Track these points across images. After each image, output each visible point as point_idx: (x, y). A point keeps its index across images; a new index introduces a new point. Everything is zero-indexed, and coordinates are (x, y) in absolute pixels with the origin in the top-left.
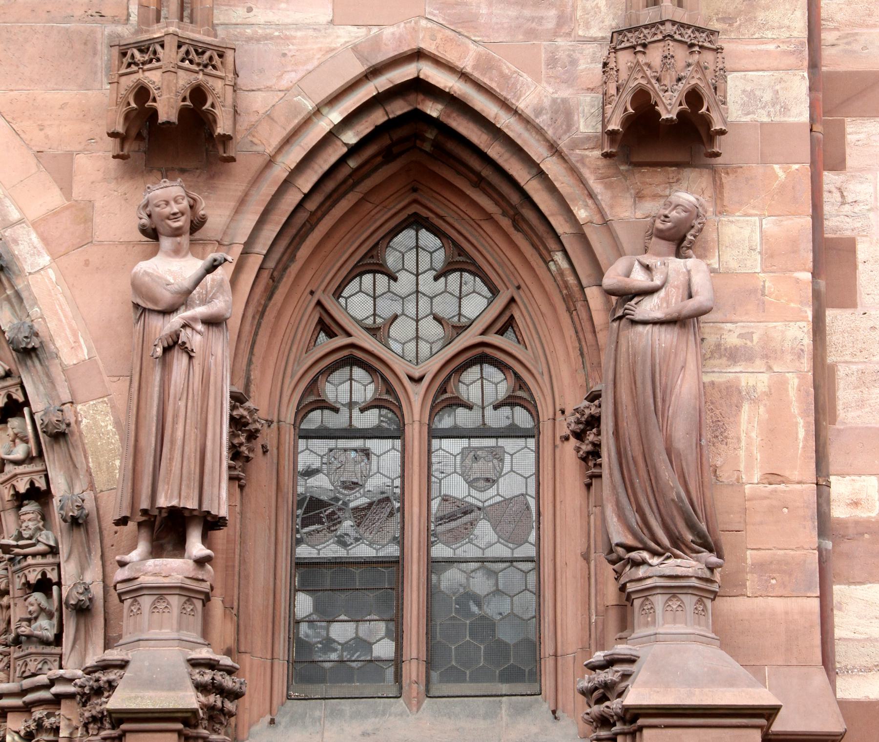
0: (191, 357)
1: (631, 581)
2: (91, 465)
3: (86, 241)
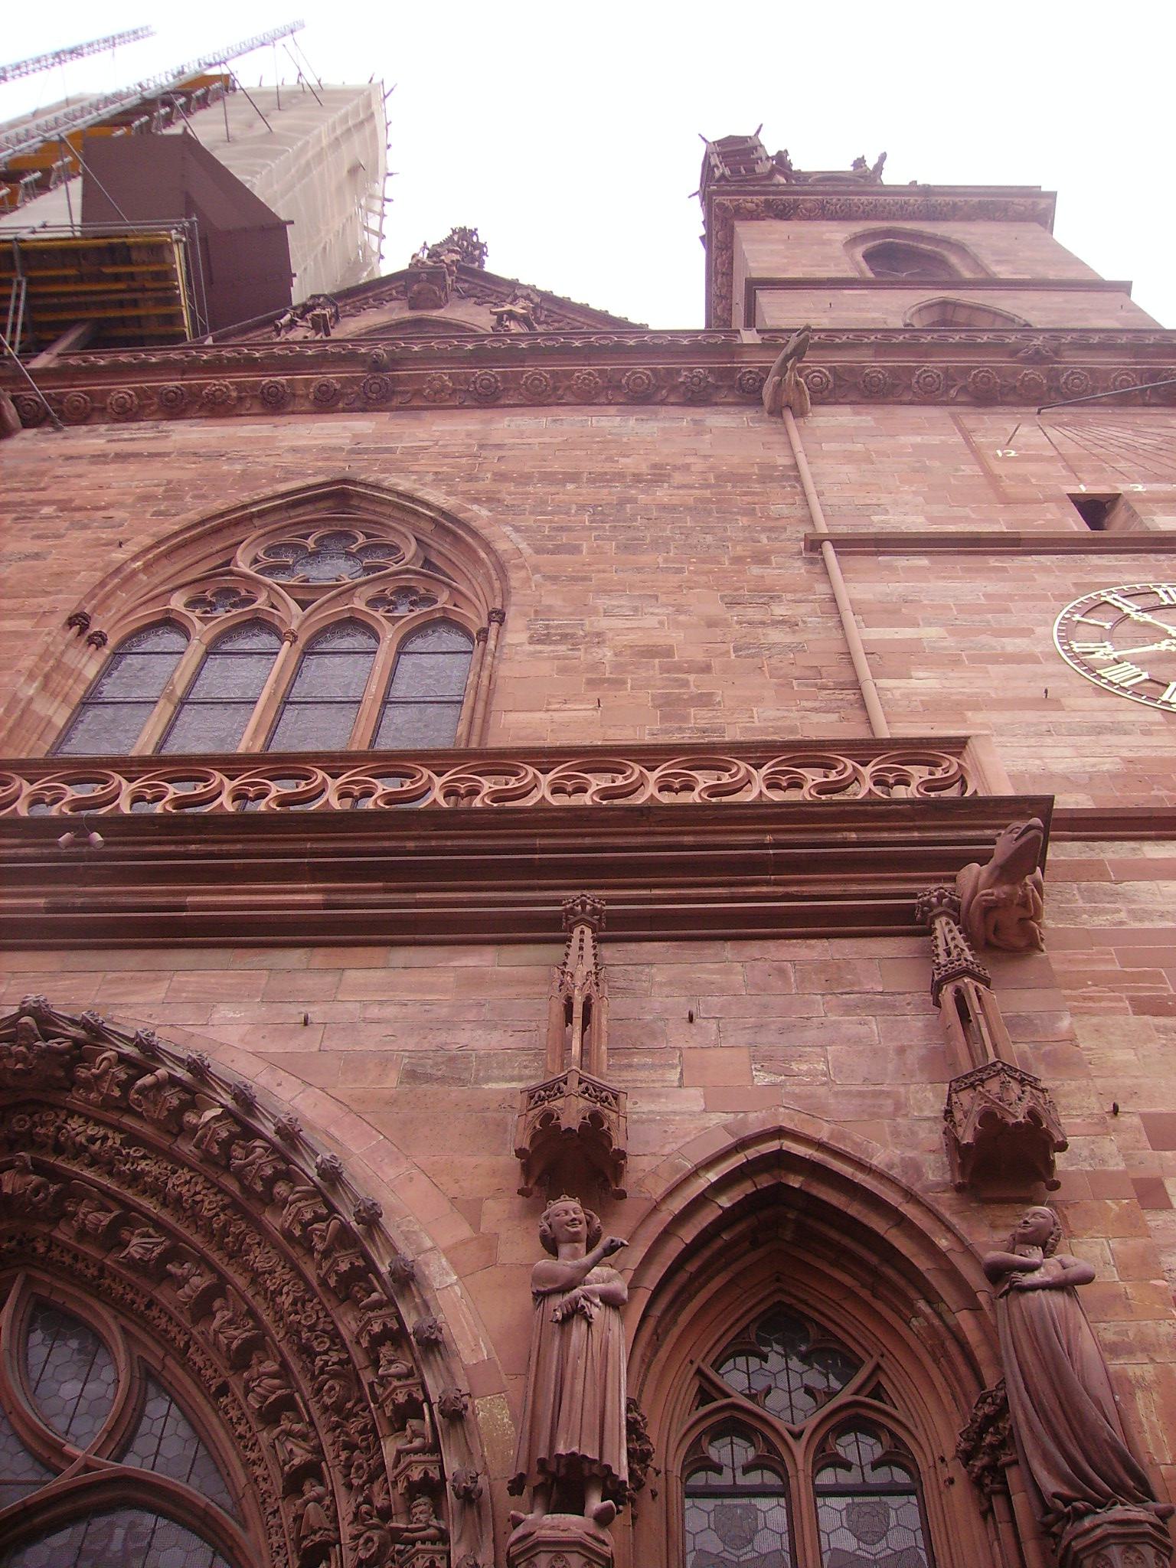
1: (1075, 1538)
2: (486, 1454)
3: (491, 1263)
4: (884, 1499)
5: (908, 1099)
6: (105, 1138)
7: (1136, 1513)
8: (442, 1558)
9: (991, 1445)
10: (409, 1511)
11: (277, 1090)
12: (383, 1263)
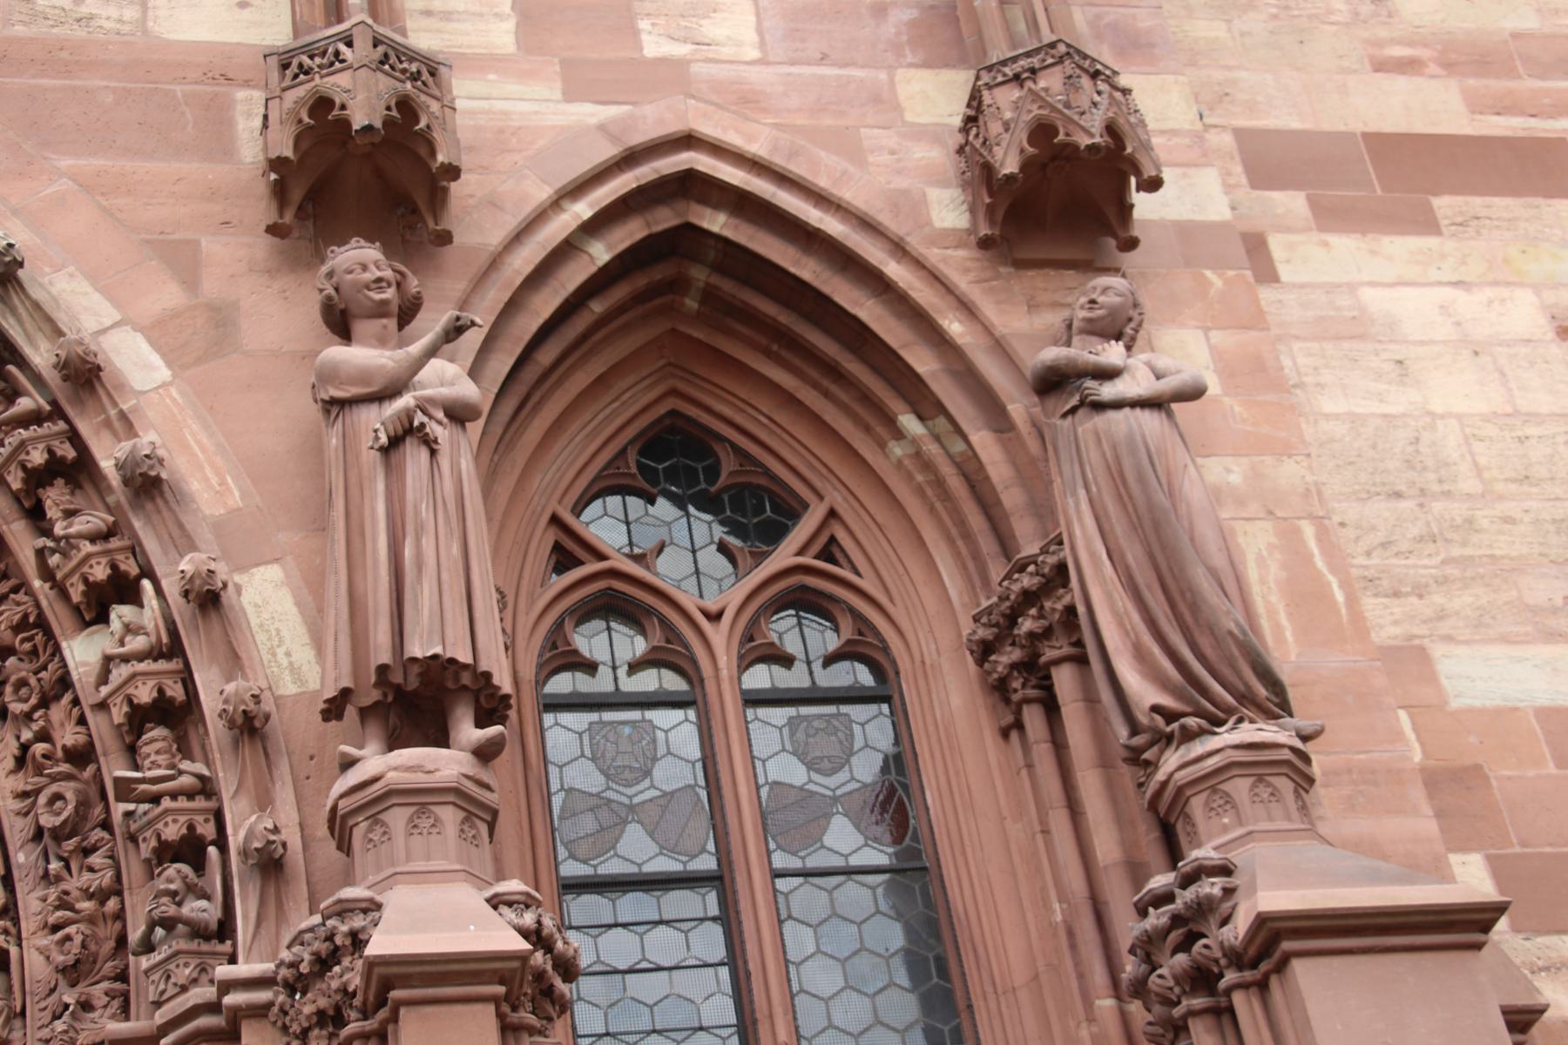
0: (433, 453)
4: (844, 709)
7: (1267, 732)
8: (206, 821)
9: (1031, 635)
10: (132, 750)
12: (36, 348)
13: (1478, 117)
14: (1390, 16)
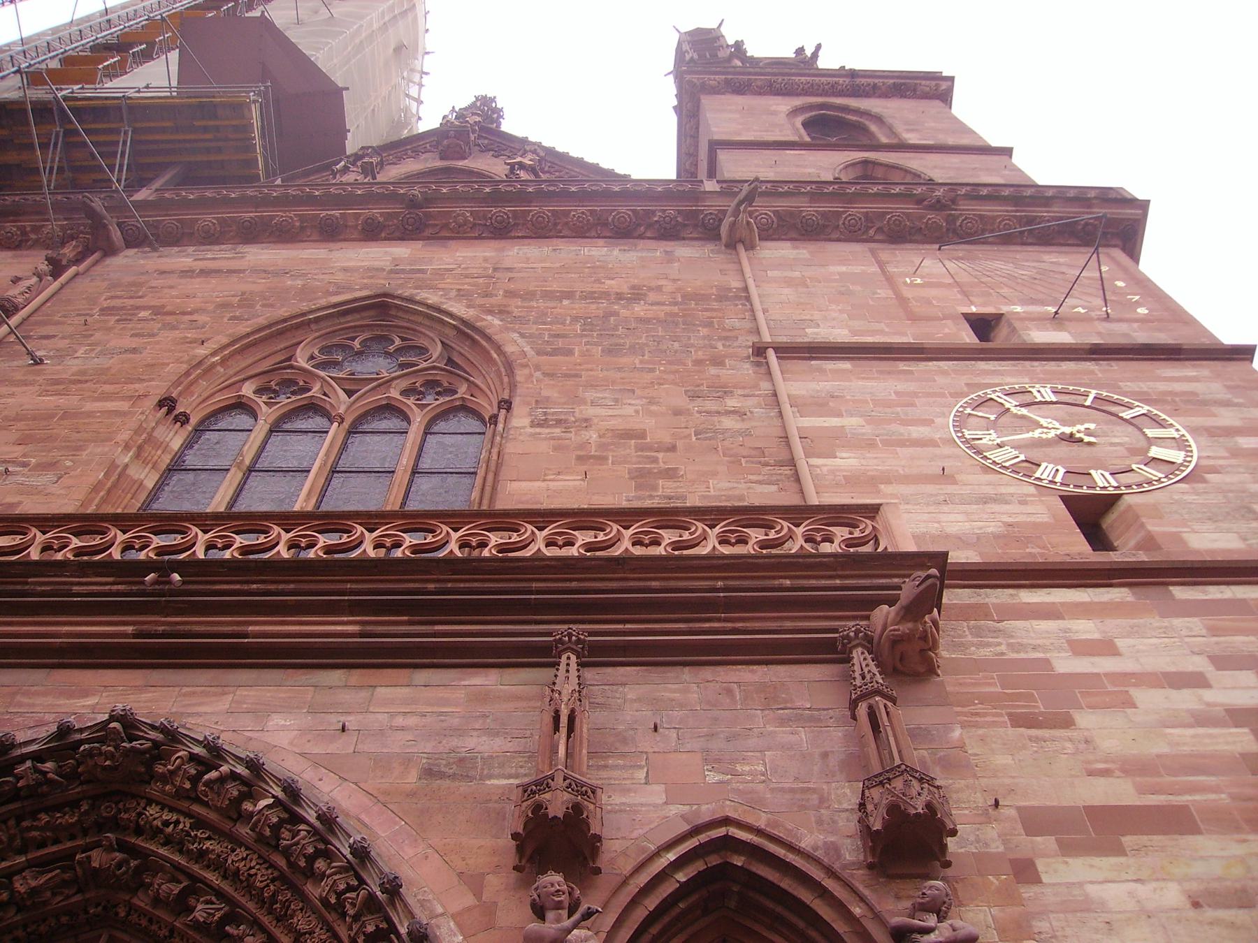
3: (490, 927)
5: (829, 794)
6: (177, 822)
11: (319, 784)
13: (1143, 796)
14: (1094, 749)
